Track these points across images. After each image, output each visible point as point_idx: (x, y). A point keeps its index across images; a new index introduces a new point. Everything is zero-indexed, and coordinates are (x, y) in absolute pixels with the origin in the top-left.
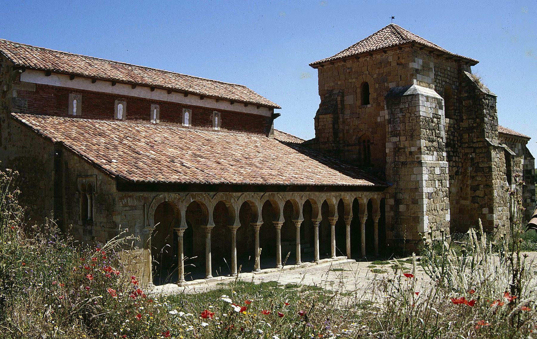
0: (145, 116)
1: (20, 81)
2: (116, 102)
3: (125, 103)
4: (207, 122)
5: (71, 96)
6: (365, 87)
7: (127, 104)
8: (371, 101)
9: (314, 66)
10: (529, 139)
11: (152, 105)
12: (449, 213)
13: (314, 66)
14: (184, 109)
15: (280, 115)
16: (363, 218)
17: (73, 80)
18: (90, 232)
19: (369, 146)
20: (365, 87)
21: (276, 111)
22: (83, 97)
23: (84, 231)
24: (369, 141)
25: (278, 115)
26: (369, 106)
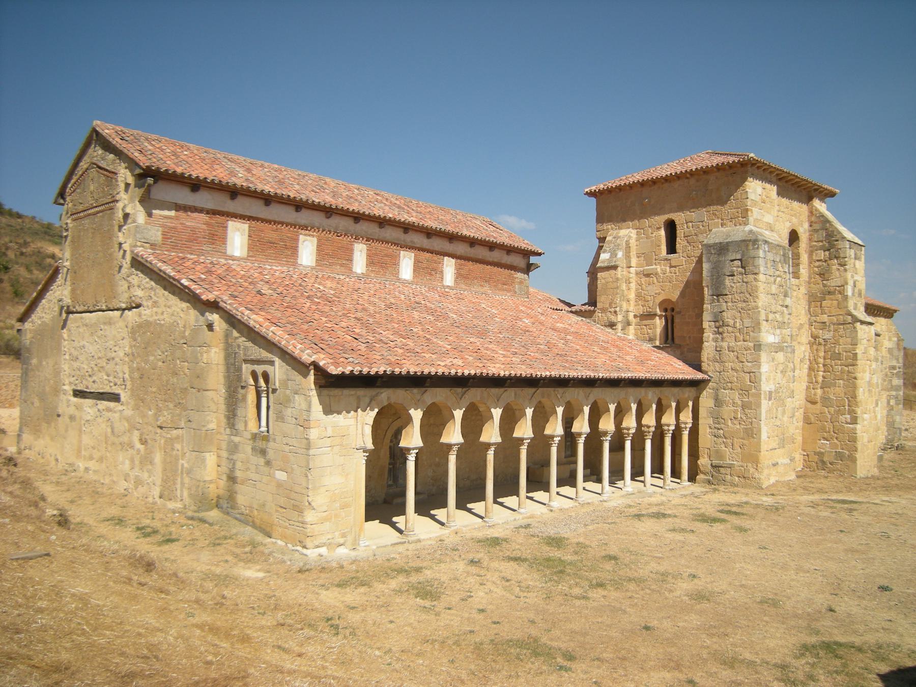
1: (149, 198)
2: (301, 238)
3: (315, 240)
7: (319, 240)
9: (591, 194)
10: (895, 311)
17: (236, 201)
18: (263, 452)
21: (533, 259)
22: (250, 227)
23: (253, 449)
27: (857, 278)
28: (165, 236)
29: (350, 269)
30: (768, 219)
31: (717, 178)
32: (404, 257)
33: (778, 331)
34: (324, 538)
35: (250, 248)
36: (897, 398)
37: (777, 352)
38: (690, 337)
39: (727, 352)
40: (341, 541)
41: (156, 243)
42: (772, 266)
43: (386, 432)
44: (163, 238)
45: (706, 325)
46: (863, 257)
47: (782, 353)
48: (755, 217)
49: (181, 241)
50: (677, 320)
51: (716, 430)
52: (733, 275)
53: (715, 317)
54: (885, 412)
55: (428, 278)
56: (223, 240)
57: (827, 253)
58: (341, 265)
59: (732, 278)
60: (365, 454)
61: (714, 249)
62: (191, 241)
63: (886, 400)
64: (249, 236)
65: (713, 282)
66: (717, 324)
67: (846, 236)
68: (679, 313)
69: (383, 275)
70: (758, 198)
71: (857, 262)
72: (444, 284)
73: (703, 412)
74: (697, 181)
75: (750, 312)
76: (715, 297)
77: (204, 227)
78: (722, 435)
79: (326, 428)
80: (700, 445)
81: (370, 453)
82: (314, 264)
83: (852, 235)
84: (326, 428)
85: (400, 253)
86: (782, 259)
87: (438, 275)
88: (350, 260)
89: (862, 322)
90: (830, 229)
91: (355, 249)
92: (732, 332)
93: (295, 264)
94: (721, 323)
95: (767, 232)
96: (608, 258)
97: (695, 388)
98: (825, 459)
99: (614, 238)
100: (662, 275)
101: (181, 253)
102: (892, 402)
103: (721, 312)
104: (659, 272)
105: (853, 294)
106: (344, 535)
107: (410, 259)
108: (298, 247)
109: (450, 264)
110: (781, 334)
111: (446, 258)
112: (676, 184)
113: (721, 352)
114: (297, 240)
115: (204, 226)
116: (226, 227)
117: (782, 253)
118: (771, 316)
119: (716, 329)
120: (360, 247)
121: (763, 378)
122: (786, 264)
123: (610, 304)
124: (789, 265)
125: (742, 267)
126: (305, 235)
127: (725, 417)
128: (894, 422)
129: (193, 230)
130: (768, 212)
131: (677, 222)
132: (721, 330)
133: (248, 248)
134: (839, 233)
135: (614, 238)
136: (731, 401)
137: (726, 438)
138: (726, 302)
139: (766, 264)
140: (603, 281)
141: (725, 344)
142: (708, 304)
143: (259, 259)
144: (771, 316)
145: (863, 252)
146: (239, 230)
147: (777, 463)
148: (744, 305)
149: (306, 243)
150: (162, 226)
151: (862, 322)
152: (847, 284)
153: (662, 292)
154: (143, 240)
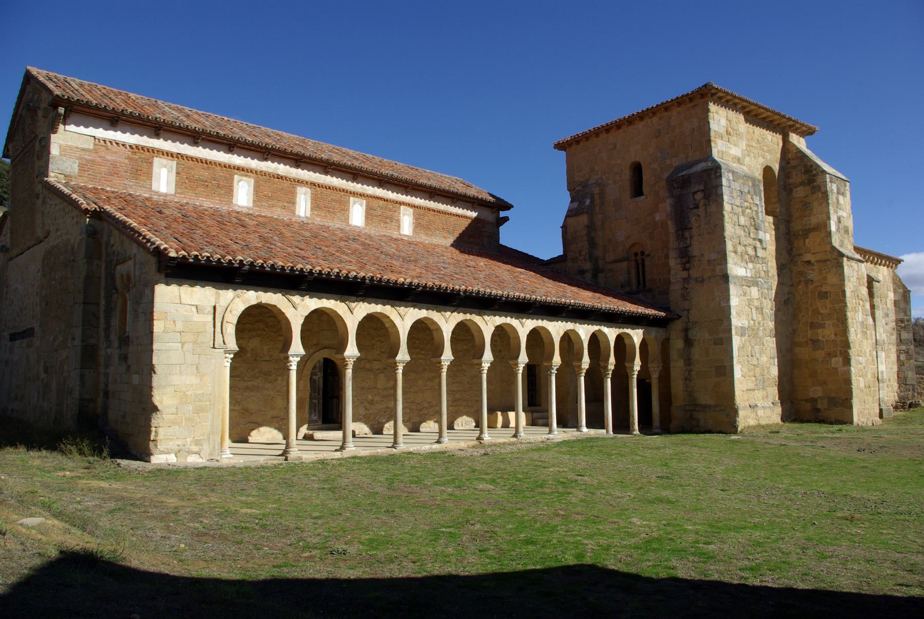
0: (285, 204)
2: (236, 176)
3: (252, 181)
4: (392, 222)
5: (157, 161)
6: (637, 169)
7: (255, 182)
8: (645, 189)
9: (560, 146)
11: (299, 188)
12: (776, 363)
13: (560, 146)
14: (352, 199)
15: (508, 220)
19: (643, 260)
20: (637, 169)
21: (502, 214)
22: (178, 164)
24: (643, 253)
25: (506, 219)
26: (642, 198)
27: (841, 213)
28: (82, 168)
29: (295, 214)
30: (735, 151)
31: (678, 113)
32: (354, 203)
33: (750, 265)
34: (171, 443)
35: (178, 184)
36: (908, 353)
37: (749, 287)
38: (660, 280)
40: (195, 448)
41: (72, 174)
42: (739, 196)
43: (306, 363)
44: (79, 170)
45: (672, 262)
46: (848, 194)
47: (756, 289)
48: (719, 148)
49: (101, 174)
50: (647, 263)
54: (895, 368)
55: (382, 225)
56: (149, 175)
57: (808, 188)
58: (284, 208)
60: (227, 355)
62: (112, 175)
63: (896, 355)
64: (177, 173)
67: (825, 169)
68: (649, 255)
69: (330, 220)
70: (722, 131)
71: (841, 198)
72: (401, 233)
73: (674, 354)
74: (660, 119)
77: (127, 161)
79: (174, 322)
81: (234, 354)
82: (251, 205)
83: (834, 170)
84: (174, 322)
85: (349, 199)
86: (752, 190)
87: (393, 224)
88: (293, 202)
89: (849, 258)
90: (809, 164)
91: (298, 191)
93: (230, 202)
95: (735, 165)
96: (575, 207)
97: (665, 329)
98: (819, 406)
99: (583, 187)
101: (100, 185)
102: (903, 357)
105: (838, 230)
106: (197, 443)
107: (362, 206)
108: (233, 186)
109: (407, 213)
110: (754, 268)
111: (402, 207)
112: (640, 125)
114: (233, 179)
115: (127, 161)
116: (151, 163)
117: (750, 184)
118: (740, 249)
120: (304, 191)
121: (733, 312)
122: (756, 195)
124: (760, 197)
126: (242, 175)
128: (905, 379)
129: (114, 164)
130: (735, 145)
131: (642, 165)
133: (176, 184)
134: (818, 166)
135: (583, 187)
139: (731, 193)
143: (188, 197)
144: (740, 249)
145: (848, 188)
146: (165, 167)
147: (757, 406)
149: (241, 183)
150: (80, 158)
151: (849, 258)
152: (829, 218)
154: (57, 171)
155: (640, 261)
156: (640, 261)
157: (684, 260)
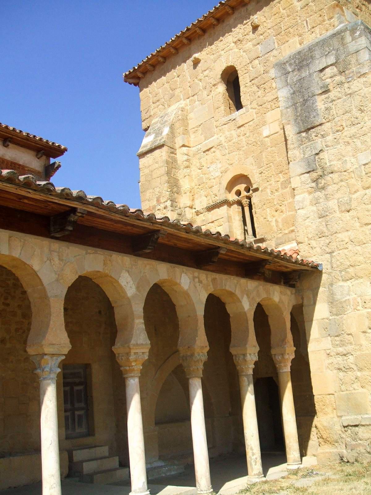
16: (245, 355)
39: (338, 214)
50: (255, 200)
51: (340, 359)
52: (326, 91)
53: (309, 164)
59: (326, 95)
61: (290, 65)
65: (297, 112)
66: (314, 175)
75: (365, 138)
76: (304, 134)
78: (353, 366)
80: (315, 392)
92: (342, 181)
94: (320, 172)
100: (226, 145)
103: (317, 154)
104: (223, 142)
113: (328, 218)
119: (314, 185)
123: (158, 200)
125: (341, 73)
127: (353, 330)
132: (322, 182)
136: (359, 300)
137: (360, 370)
138: (323, 136)
140: (147, 171)
141: (332, 204)
142: (294, 148)
148: (353, 130)
153: (230, 167)
155: (245, 202)
156: (245, 202)
157: (314, 175)
